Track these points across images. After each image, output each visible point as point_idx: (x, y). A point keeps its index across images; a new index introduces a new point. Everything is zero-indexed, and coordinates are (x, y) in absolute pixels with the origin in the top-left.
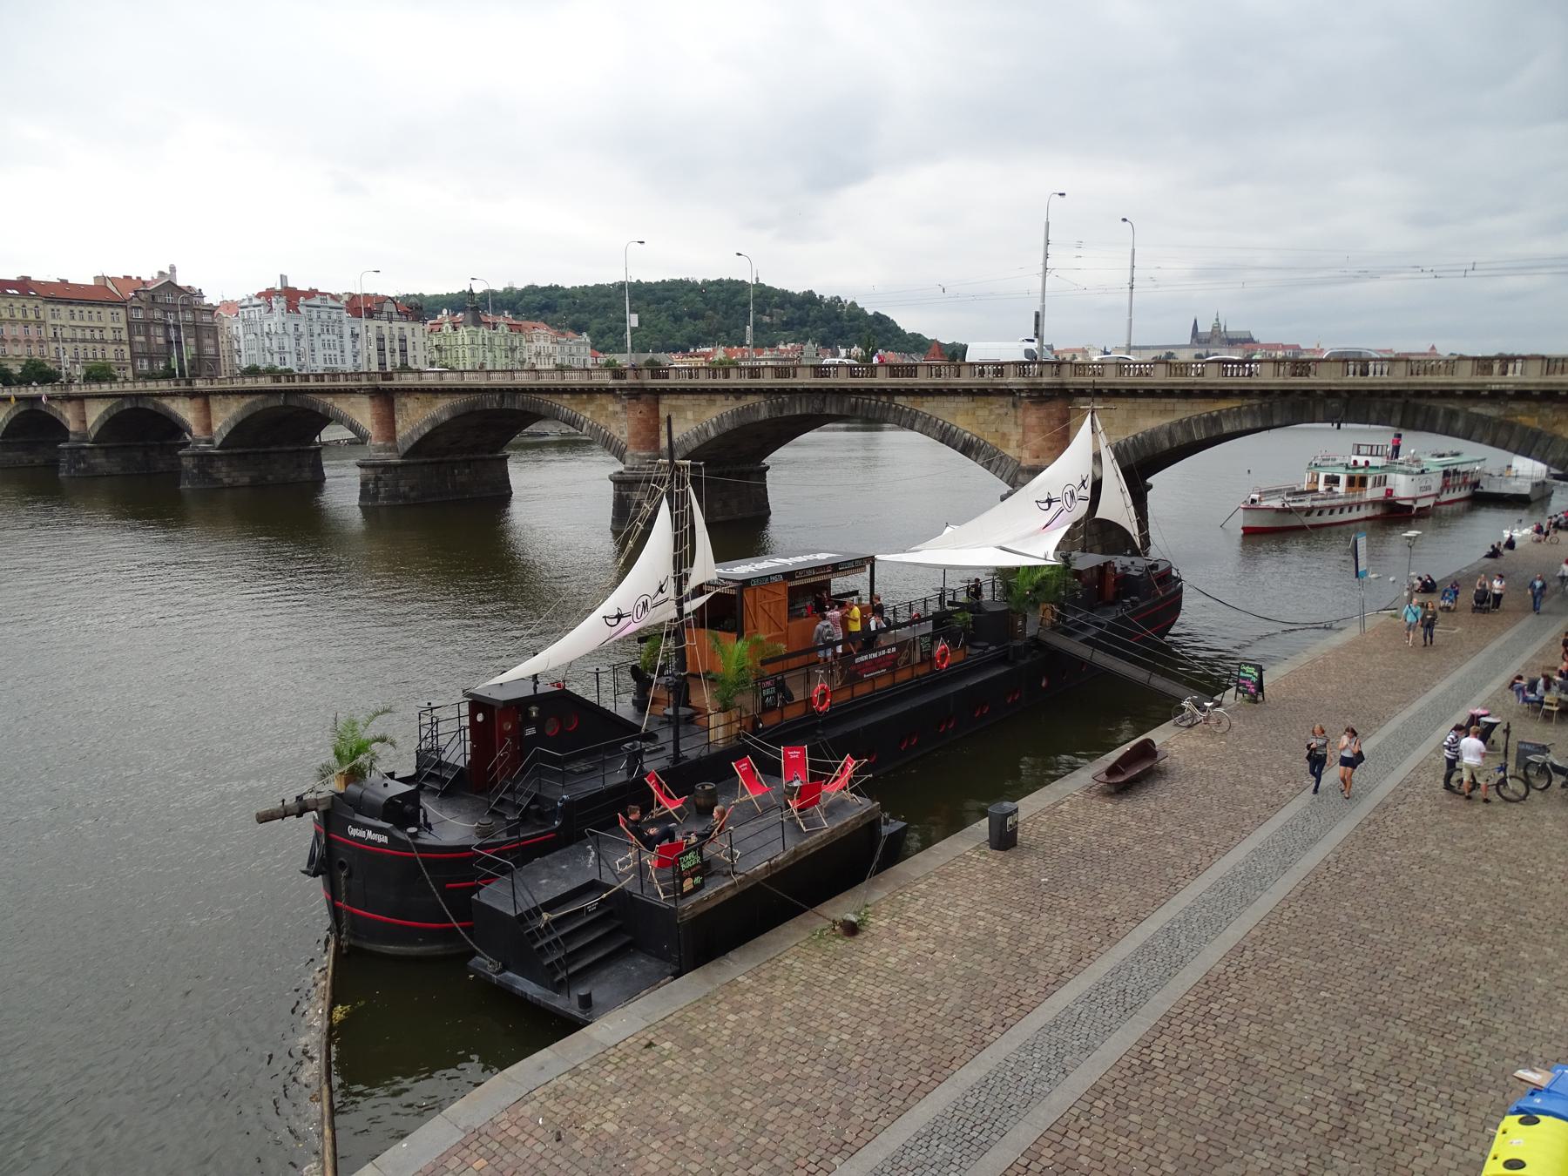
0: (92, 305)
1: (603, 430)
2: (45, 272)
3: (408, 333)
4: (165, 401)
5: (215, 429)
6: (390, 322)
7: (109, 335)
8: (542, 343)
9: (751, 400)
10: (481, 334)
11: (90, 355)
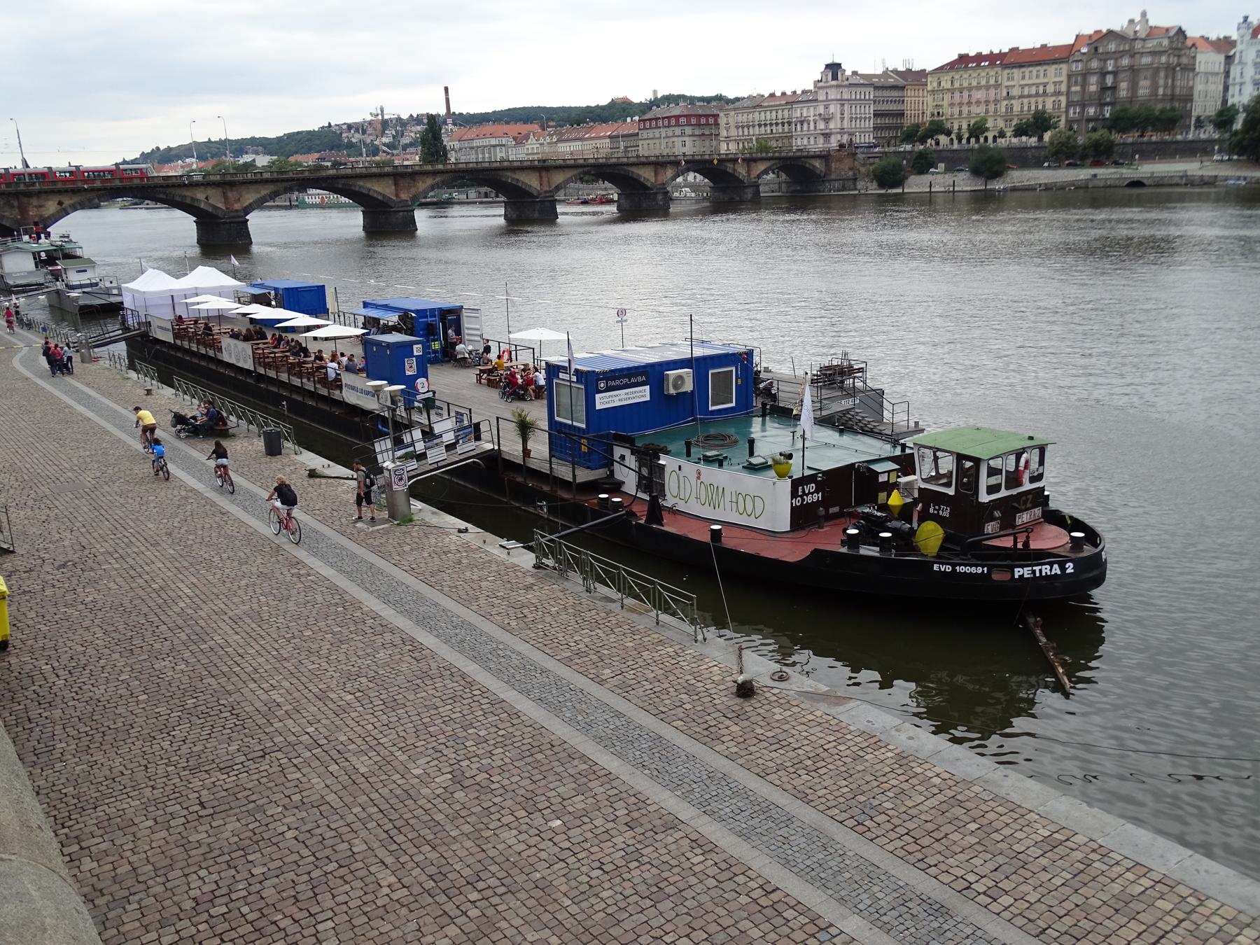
0: (1040, 64)
4: (635, 170)
11: (1026, 108)
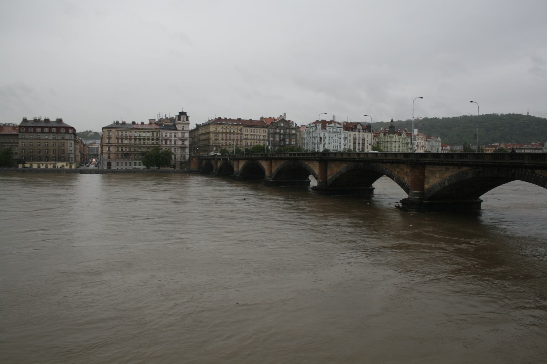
0: (258, 127)
1: (402, 180)
2: (245, 117)
3: (366, 137)
5: (273, 172)
6: (359, 133)
7: (262, 138)
8: (420, 141)
9: (465, 168)
10: (394, 137)
